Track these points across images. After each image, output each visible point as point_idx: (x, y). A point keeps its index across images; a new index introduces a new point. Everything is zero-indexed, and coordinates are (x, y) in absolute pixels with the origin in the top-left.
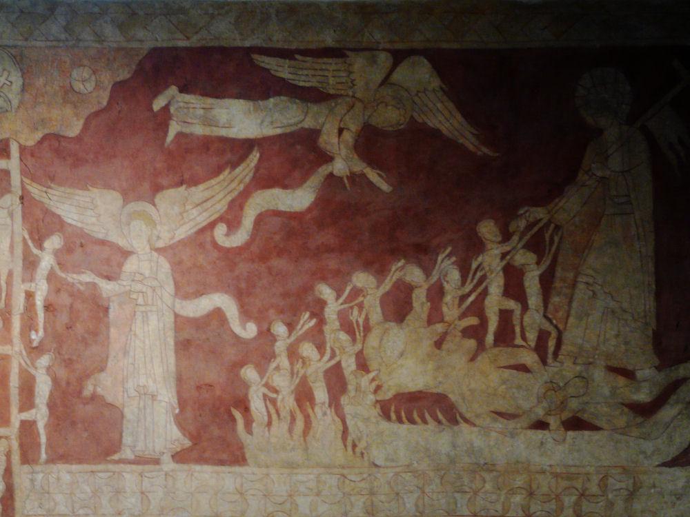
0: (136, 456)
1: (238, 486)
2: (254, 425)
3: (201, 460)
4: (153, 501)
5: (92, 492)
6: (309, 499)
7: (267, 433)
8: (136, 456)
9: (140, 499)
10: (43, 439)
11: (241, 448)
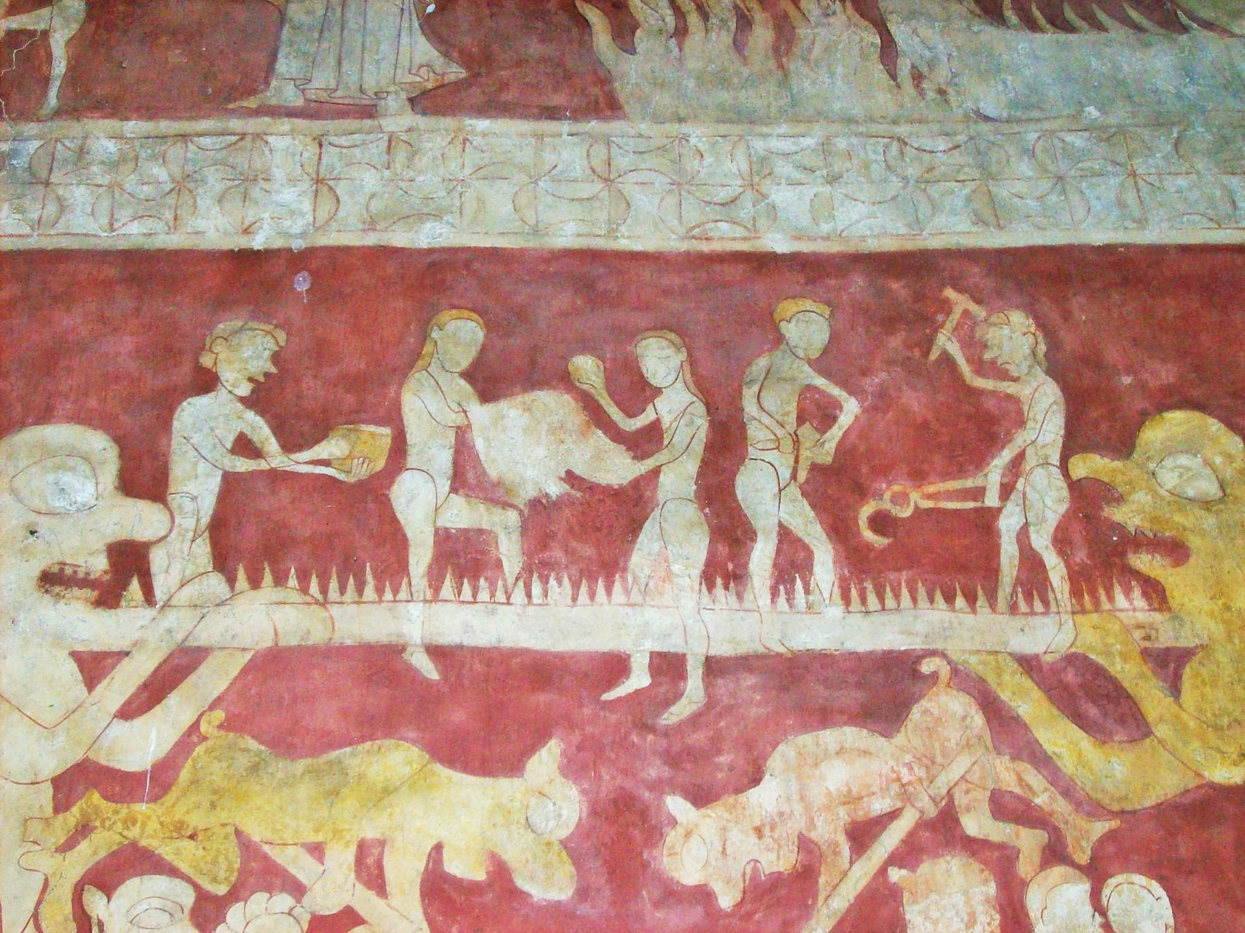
0: (308, 101)
1: (598, 164)
2: (638, 33)
3: (493, 107)
4: (344, 198)
5: (173, 181)
6: (808, 192)
7: (676, 50)
8: (308, 101)
9: (311, 195)
10: (59, 68)
11: (604, 80)
